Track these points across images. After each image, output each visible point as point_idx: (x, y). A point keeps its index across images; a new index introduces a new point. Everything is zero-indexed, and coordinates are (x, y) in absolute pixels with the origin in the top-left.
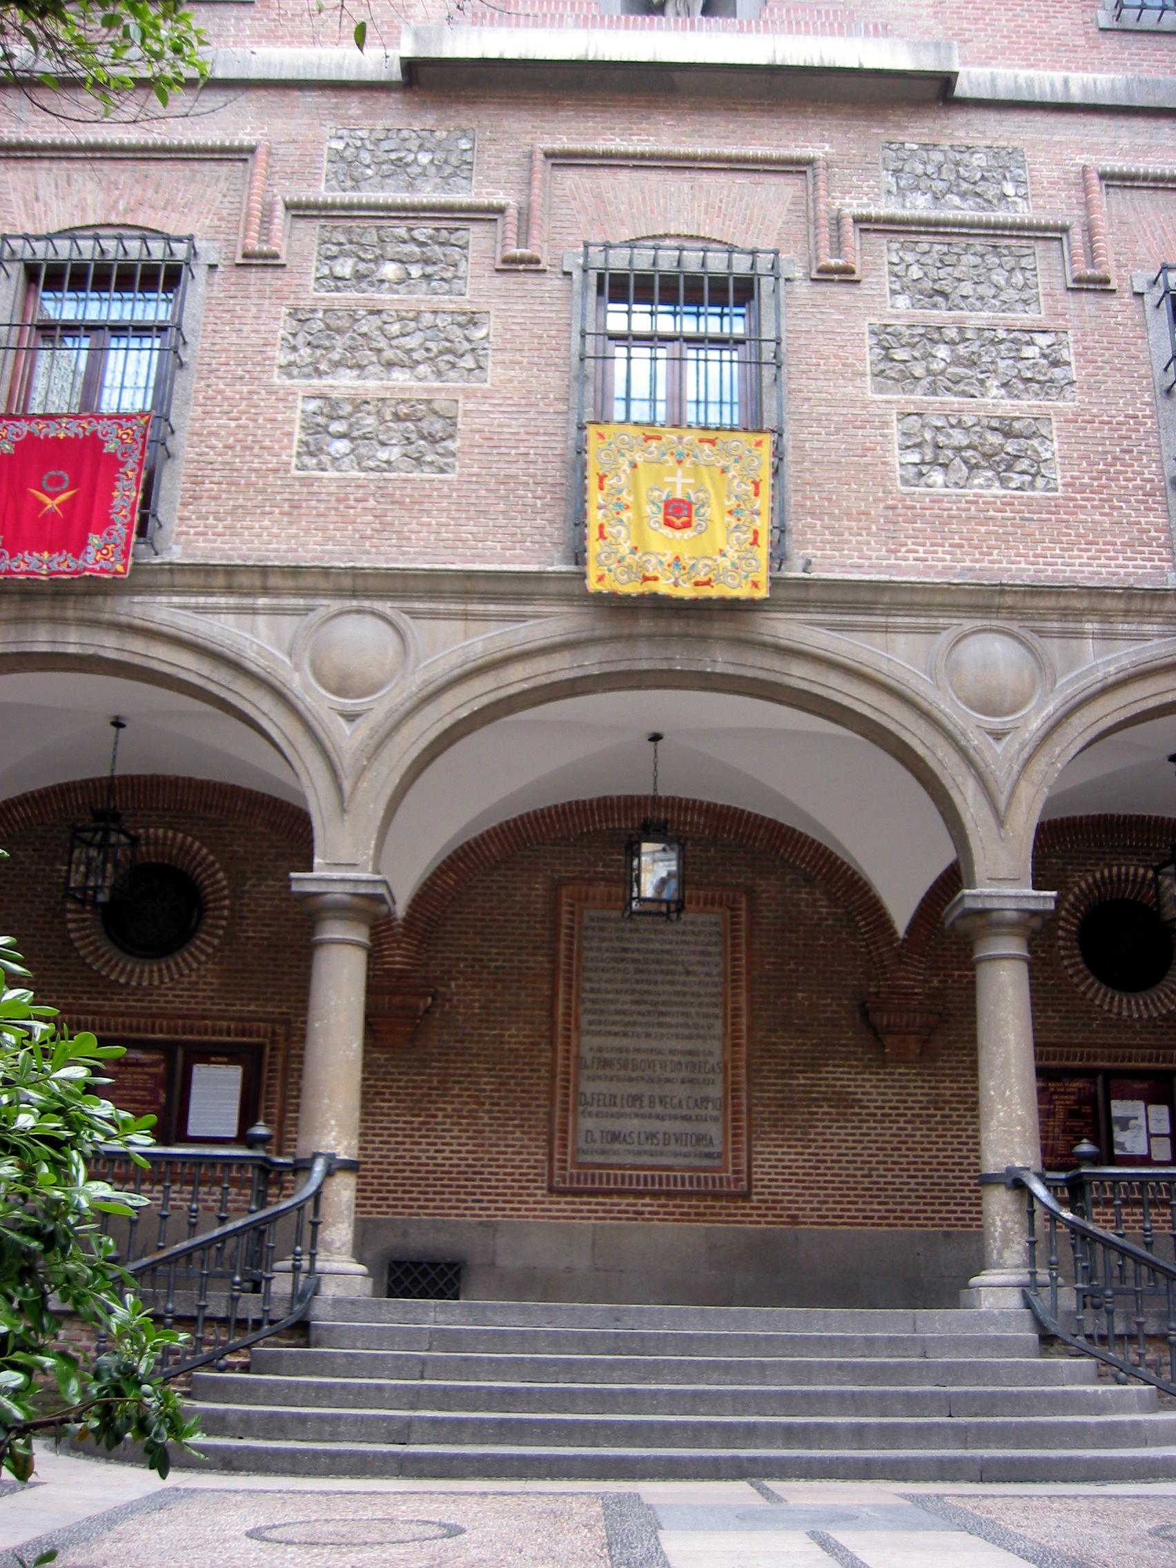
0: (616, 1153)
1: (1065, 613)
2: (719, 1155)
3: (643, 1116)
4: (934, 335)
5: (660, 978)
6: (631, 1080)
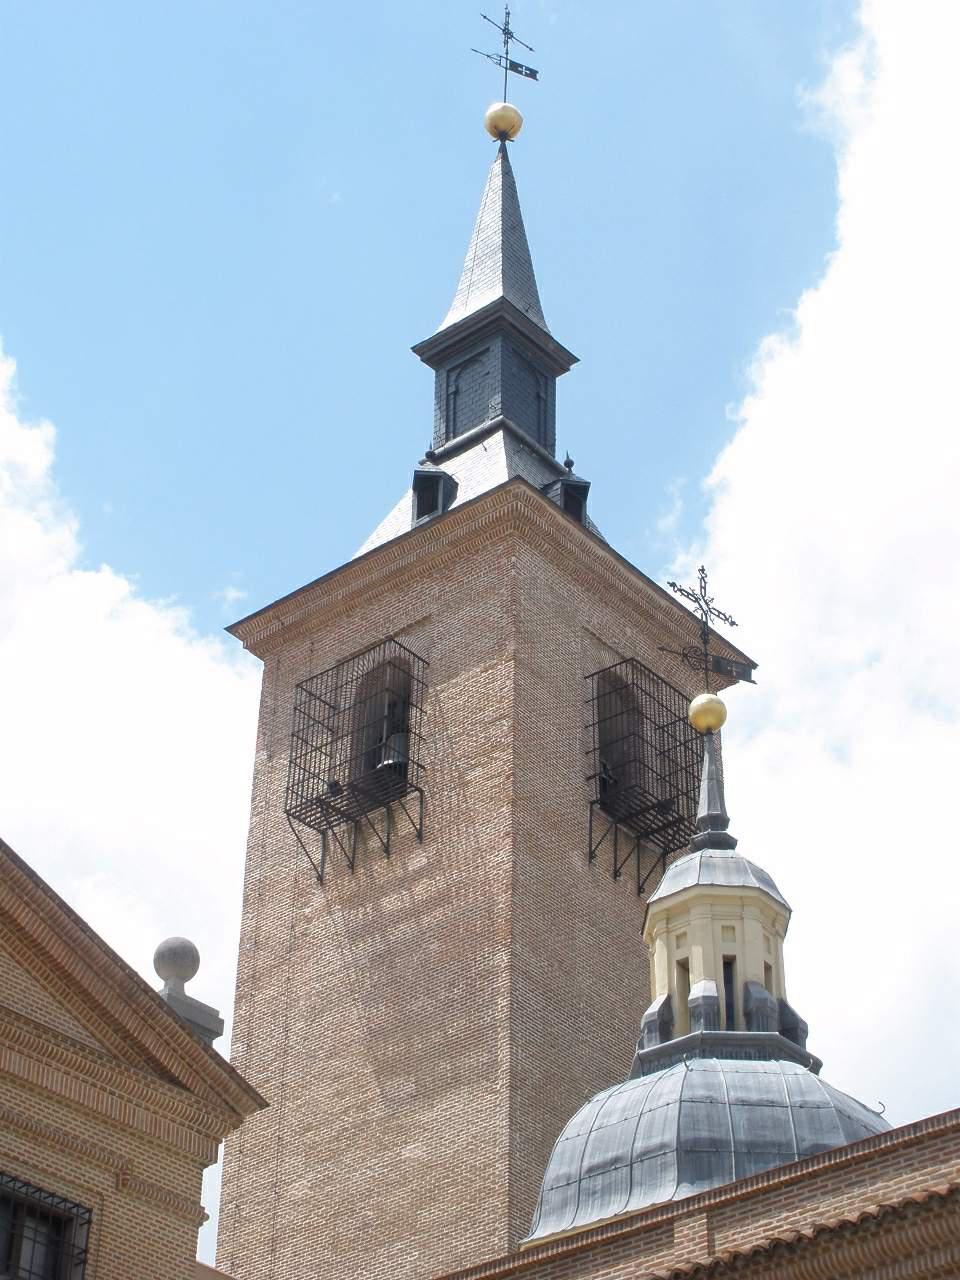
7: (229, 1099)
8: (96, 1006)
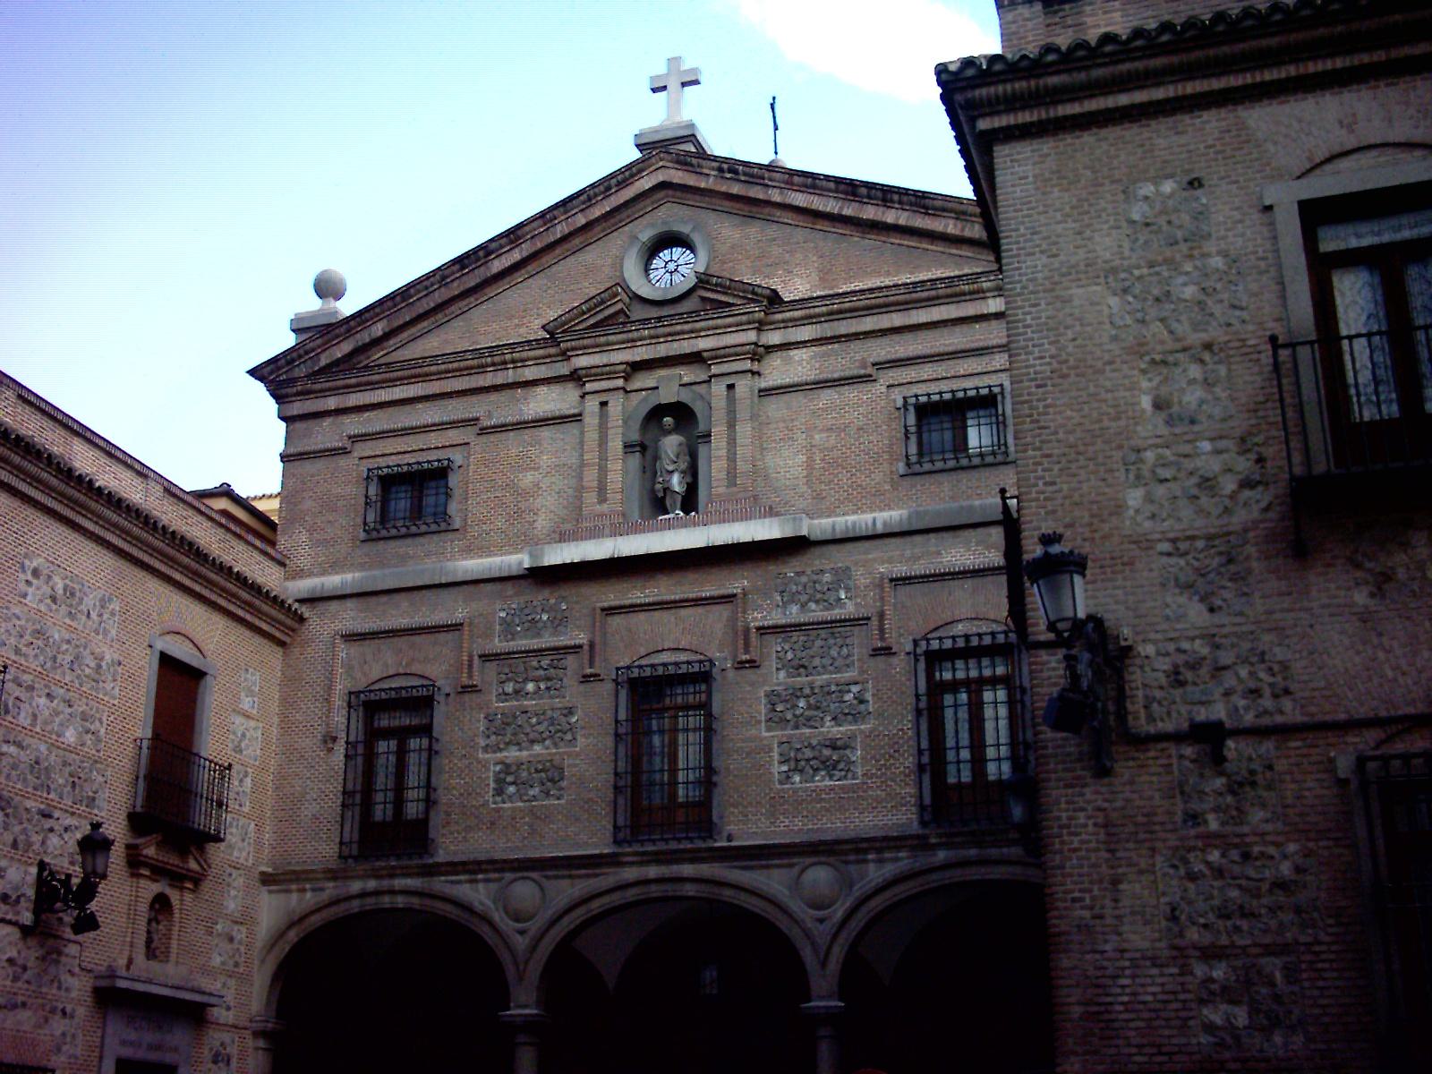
1: (857, 851)
4: (797, 693)
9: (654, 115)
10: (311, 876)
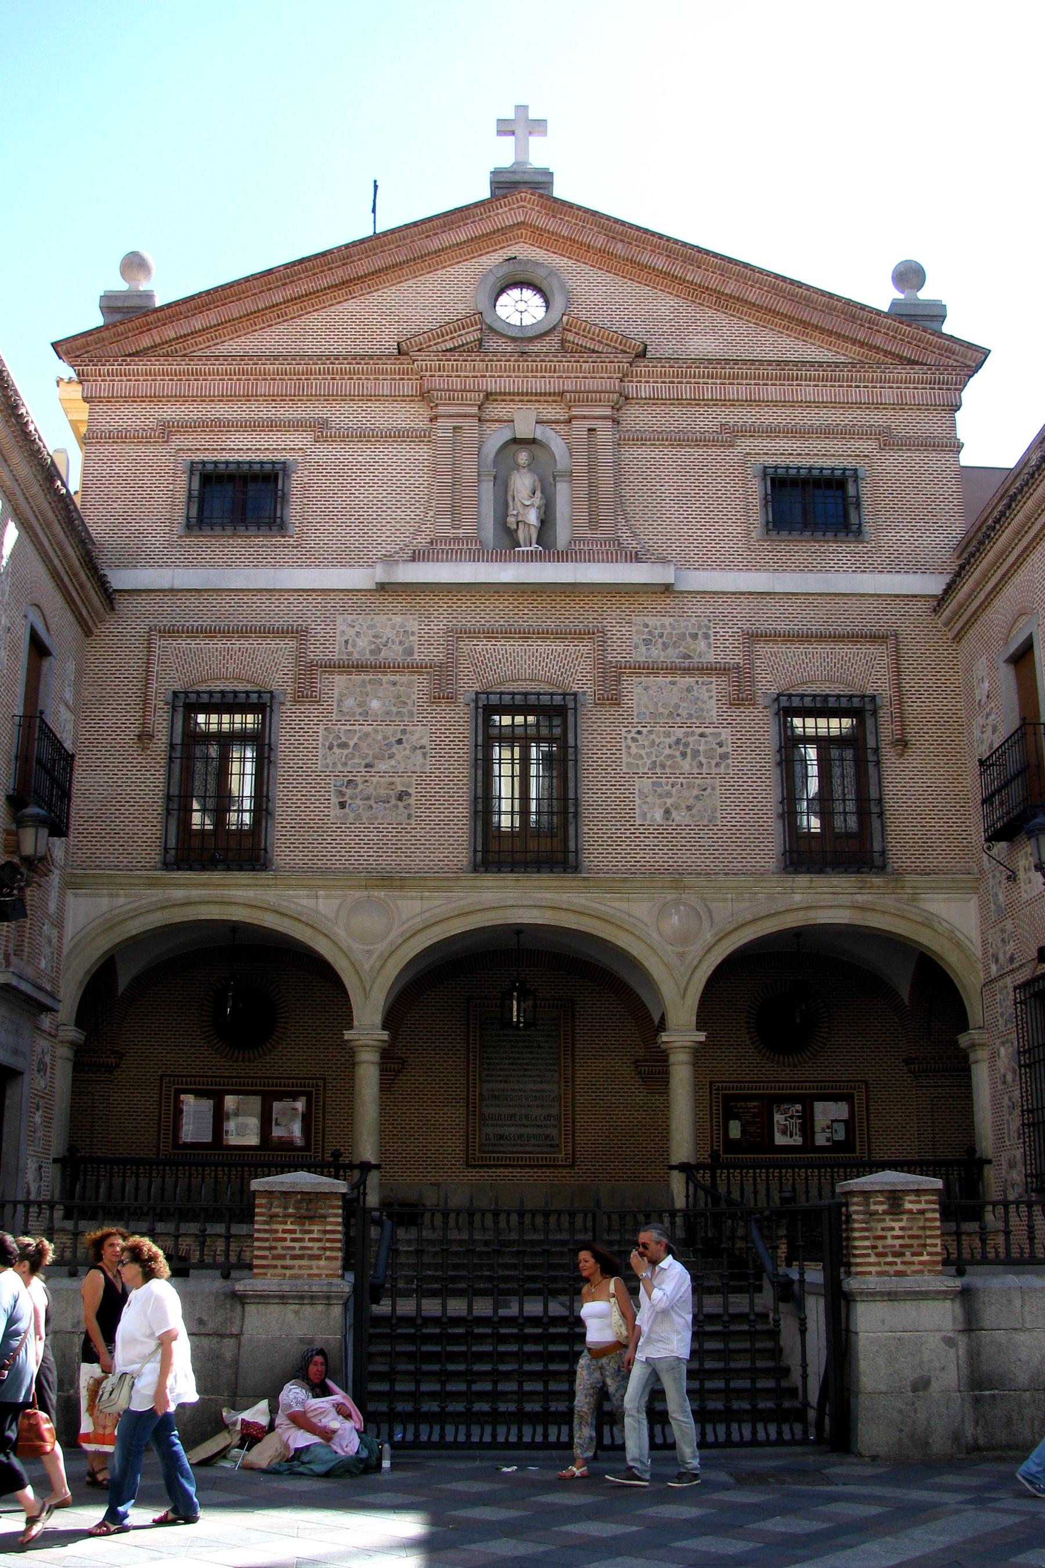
0: (502, 1145)
2: (557, 1145)
3: (516, 1125)
5: (525, 1050)
6: (510, 1106)
7: (958, 358)
8: (830, 333)
9: (503, 154)
10: (146, 881)
